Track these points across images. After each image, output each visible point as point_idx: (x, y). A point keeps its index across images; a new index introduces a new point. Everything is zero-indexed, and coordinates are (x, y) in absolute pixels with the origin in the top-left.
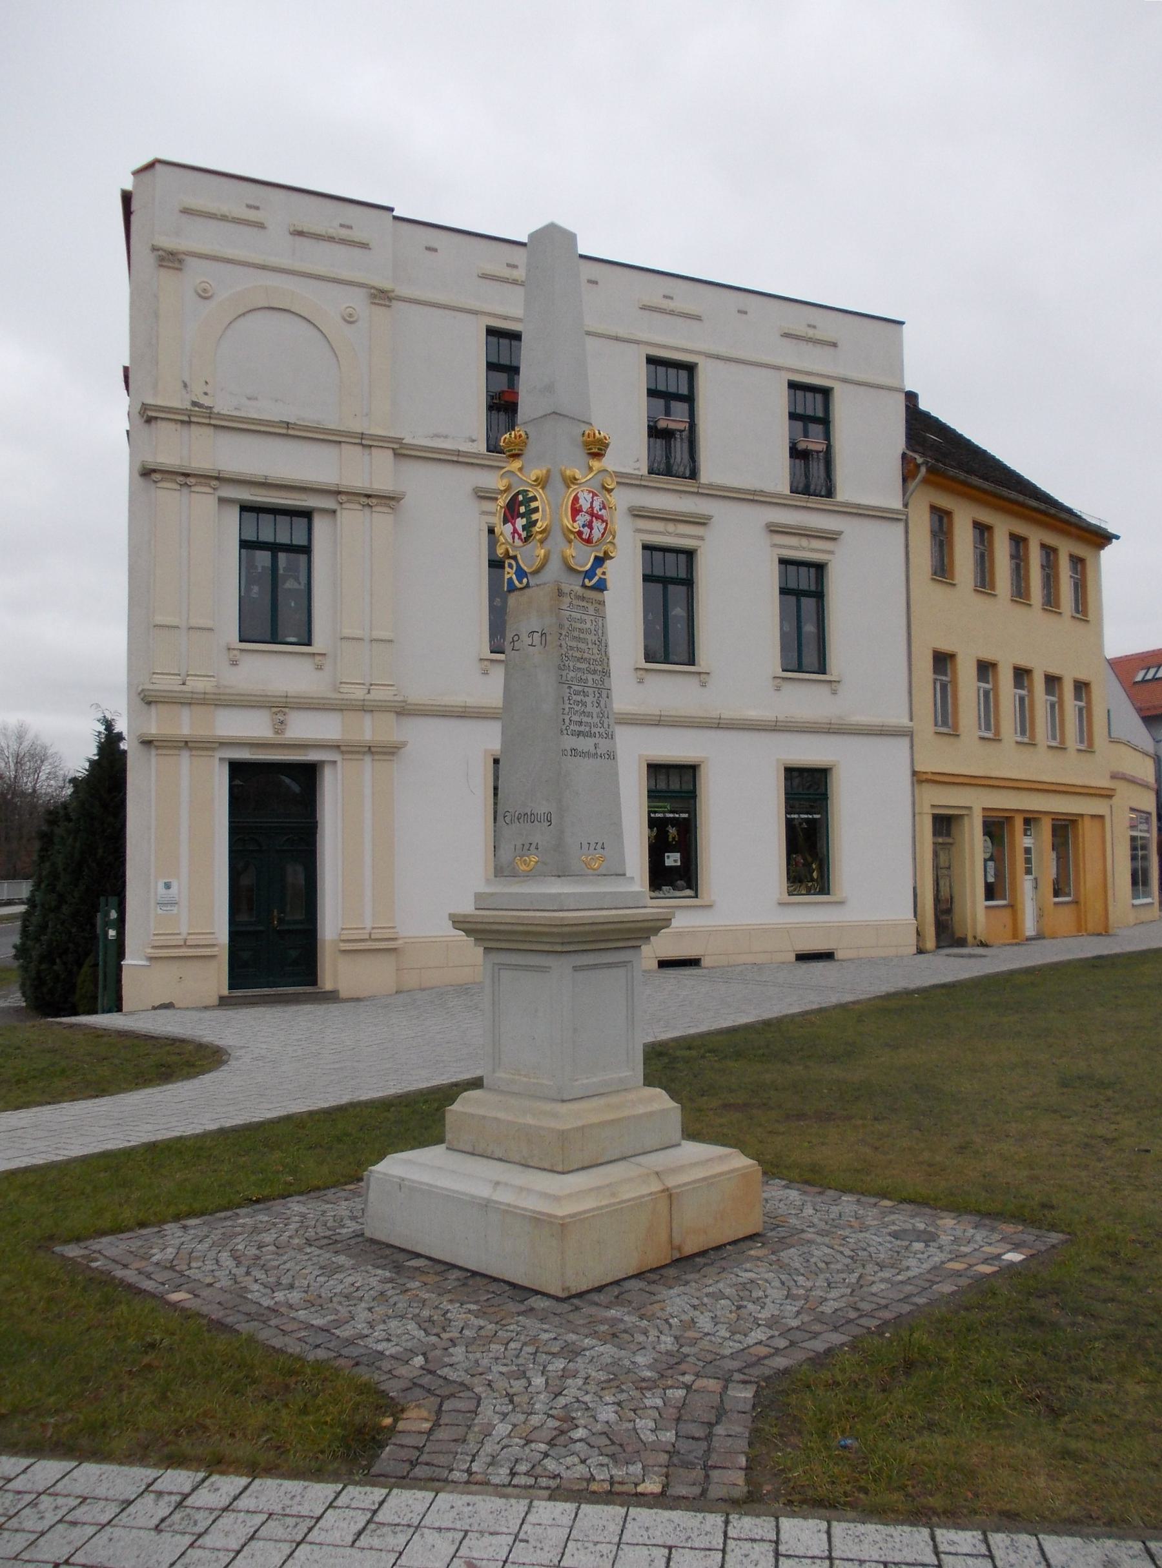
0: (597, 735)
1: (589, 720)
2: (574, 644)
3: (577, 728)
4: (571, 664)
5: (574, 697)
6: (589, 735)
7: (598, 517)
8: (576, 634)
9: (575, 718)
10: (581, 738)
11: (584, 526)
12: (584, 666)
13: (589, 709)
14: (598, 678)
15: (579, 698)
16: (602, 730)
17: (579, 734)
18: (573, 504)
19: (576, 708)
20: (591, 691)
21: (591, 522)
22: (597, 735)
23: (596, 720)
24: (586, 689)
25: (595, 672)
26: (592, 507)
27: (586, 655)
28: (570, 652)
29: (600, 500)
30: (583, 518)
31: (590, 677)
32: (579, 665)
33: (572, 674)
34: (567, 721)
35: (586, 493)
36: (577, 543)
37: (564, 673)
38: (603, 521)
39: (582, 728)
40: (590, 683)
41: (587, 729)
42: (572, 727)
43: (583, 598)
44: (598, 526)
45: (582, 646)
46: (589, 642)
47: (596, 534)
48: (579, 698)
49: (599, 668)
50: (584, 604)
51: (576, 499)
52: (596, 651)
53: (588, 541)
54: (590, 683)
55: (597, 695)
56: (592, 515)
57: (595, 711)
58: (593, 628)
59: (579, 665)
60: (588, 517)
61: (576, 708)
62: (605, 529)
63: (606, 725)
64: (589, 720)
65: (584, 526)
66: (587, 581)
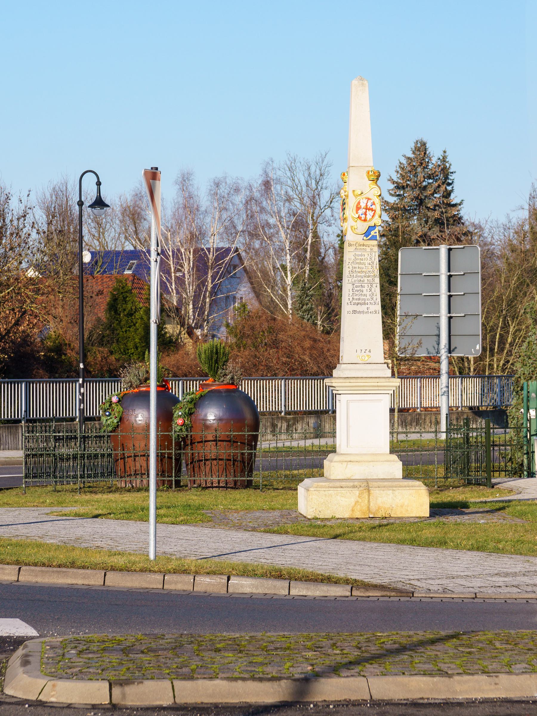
0: (369, 304)
1: (365, 297)
2: (357, 266)
3: (357, 302)
4: (355, 275)
5: (356, 289)
6: (365, 304)
7: (369, 209)
8: (358, 261)
9: (355, 297)
10: (359, 306)
11: (362, 214)
12: (363, 275)
13: (365, 292)
14: (371, 279)
15: (358, 289)
16: (372, 301)
17: (358, 304)
18: (357, 205)
19: (357, 293)
20: (366, 285)
21: (366, 212)
22: (369, 304)
23: (368, 297)
24: (363, 285)
25: (369, 276)
26: (367, 205)
27: (364, 270)
28: (354, 270)
29: (372, 201)
30: (361, 212)
31: (366, 279)
32: (359, 274)
33: (356, 279)
34: (351, 299)
35: (364, 199)
36: (359, 220)
37: (350, 279)
38: (372, 210)
39: (359, 302)
40: (366, 281)
41: (363, 301)
42: (354, 301)
43: (363, 245)
44: (370, 214)
45: (363, 266)
46: (366, 264)
47: (369, 217)
48: (358, 289)
49: (372, 274)
50: (364, 247)
51: (359, 203)
52: (370, 267)
53: (365, 220)
54: (366, 281)
55: (370, 286)
56: (366, 209)
57: (368, 293)
58: (369, 258)
59: (359, 274)
60: (364, 210)
61: (357, 293)
62: (374, 214)
63: (374, 299)
64: (365, 297)
65: (362, 214)
66: (365, 238)
